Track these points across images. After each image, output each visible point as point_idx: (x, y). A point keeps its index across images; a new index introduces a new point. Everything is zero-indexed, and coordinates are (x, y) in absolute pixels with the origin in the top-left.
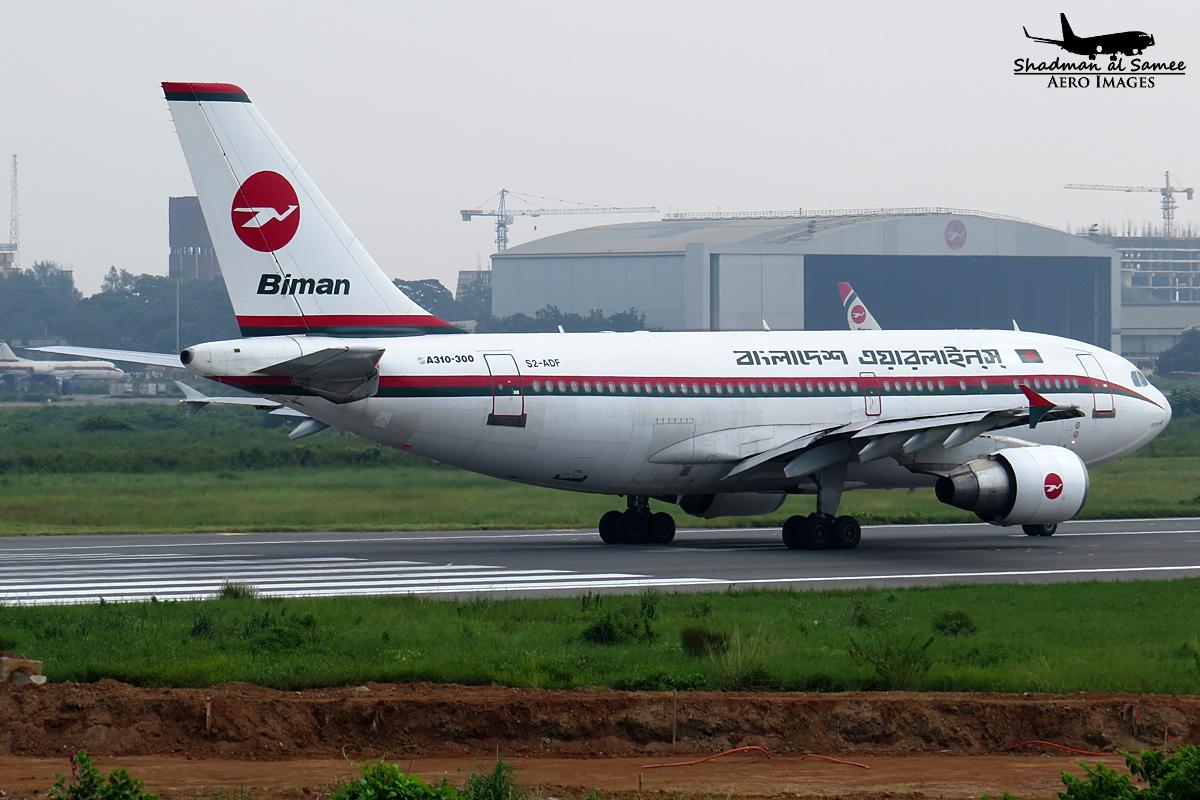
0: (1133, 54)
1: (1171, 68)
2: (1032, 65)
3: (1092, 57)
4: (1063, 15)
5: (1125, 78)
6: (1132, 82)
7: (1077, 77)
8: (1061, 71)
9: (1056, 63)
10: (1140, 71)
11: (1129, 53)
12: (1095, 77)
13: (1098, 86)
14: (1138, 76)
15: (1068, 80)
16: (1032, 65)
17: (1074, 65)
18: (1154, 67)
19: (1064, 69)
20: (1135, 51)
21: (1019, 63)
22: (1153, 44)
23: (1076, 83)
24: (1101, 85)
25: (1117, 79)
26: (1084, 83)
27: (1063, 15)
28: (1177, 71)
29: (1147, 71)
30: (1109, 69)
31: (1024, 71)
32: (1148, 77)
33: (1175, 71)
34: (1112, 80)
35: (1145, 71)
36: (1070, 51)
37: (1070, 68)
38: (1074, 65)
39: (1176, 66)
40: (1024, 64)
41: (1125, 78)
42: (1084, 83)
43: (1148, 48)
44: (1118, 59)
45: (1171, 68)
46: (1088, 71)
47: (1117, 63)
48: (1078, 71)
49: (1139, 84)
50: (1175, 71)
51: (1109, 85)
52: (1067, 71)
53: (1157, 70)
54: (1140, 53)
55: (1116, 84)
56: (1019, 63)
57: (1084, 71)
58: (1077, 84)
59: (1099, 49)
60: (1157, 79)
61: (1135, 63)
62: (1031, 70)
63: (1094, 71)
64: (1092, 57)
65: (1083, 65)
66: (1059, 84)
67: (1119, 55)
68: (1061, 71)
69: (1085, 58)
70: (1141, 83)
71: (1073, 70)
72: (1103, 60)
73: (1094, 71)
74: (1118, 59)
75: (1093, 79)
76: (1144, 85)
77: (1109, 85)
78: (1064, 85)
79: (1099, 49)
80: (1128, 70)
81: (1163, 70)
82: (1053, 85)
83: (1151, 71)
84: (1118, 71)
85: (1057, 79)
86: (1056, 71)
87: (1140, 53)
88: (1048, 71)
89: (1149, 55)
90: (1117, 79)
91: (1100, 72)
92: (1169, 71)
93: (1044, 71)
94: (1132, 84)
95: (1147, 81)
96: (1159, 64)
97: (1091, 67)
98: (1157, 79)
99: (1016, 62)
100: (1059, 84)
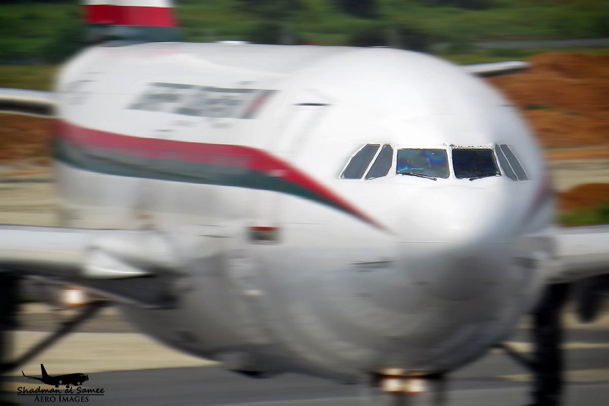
0: (77, 385)
1: (97, 392)
2: (27, 390)
3: (57, 386)
4: (42, 365)
5: (74, 397)
6: (77, 399)
7: (49, 397)
8: (41, 393)
9: (39, 389)
10: (81, 393)
11: (76, 384)
12: (58, 396)
13: (60, 401)
14: (80, 396)
15: (44, 398)
16: (27, 390)
17: (47, 390)
18: (89, 391)
19: (45, 392)
20: (79, 383)
21: (20, 389)
22: (88, 379)
23: (49, 400)
24: (62, 399)
25: (69, 397)
26: (53, 399)
27: (42, 365)
28: (100, 393)
29: (85, 393)
30: (66, 392)
31: (22, 393)
32: (85, 396)
33: (99, 394)
34: (67, 398)
35: (84, 394)
36: (46, 383)
37: (45, 392)
38: (47, 390)
39: (99, 391)
40: (22, 390)
41: (74, 397)
42: (53, 399)
43: (85, 381)
44: (70, 387)
45: (97, 392)
46: (55, 393)
47: (70, 389)
48: (50, 393)
49: (80, 400)
50: (99, 394)
51: (65, 401)
52: (44, 393)
53: (90, 393)
54: (81, 384)
55: (69, 400)
56: (20, 389)
57: (53, 393)
58: (49, 400)
59: (61, 382)
60: (90, 397)
61: (79, 389)
62: (26, 393)
63: (58, 393)
64: (57, 386)
65: (52, 390)
66: (40, 400)
67: (70, 386)
68: (41, 393)
69: (53, 387)
70: (82, 399)
71: (47, 393)
72: (62, 387)
73: (58, 393)
74: (70, 387)
75: (57, 397)
76: (83, 400)
77: (65, 401)
78: (43, 400)
79: (61, 382)
80: (75, 393)
81: (93, 393)
82: (37, 401)
83: (87, 393)
84: (70, 393)
85: (39, 397)
86: (38, 393)
87: (81, 384)
88: (35, 393)
89: (85, 386)
90: (69, 397)
91: (61, 394)
92: (96, 393)
93: (32, 393)
94: (77, 400)
95: (85, 398)
96: (91, 390)
97: (57, 391)
98: (90, 397)
99: (18, 389)
100: (40, 400)
